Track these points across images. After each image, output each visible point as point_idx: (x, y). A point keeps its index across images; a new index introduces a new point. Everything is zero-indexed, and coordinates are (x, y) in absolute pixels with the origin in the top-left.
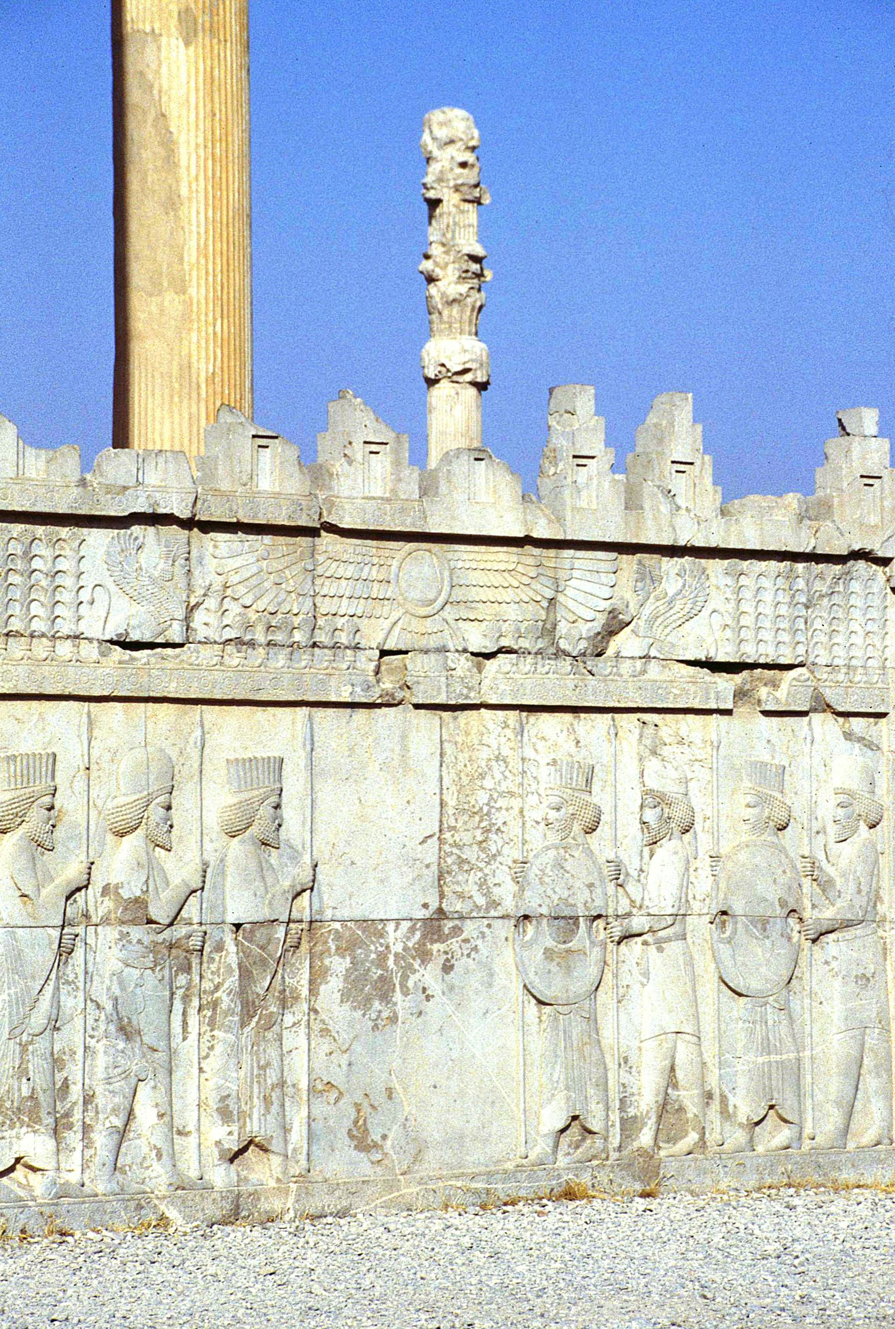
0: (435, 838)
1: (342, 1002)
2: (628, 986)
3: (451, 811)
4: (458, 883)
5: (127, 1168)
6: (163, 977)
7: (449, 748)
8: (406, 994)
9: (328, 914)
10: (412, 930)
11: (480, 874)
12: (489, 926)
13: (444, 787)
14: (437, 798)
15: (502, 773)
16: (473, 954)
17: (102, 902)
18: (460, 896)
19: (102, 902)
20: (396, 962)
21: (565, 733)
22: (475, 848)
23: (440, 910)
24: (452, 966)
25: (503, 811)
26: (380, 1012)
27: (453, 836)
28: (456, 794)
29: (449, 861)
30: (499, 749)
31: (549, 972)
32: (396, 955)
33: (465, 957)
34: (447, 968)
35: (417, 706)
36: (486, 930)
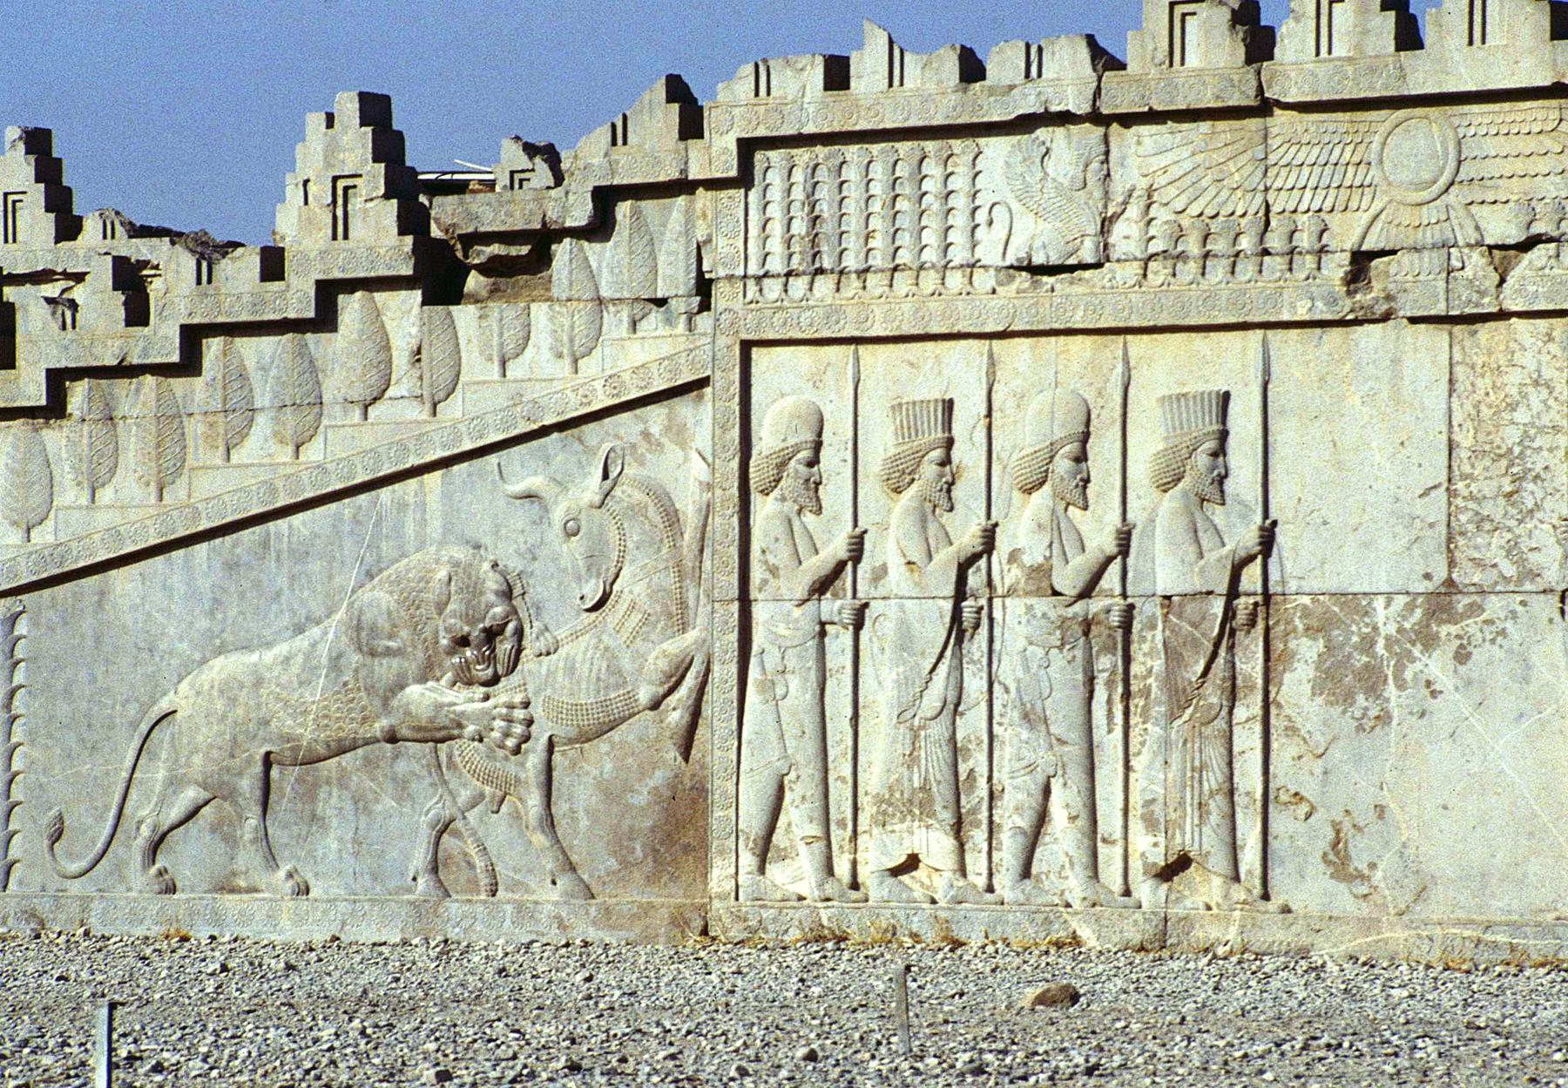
0: (1443, 489)
1: (1314, 694)
3: (1464, 454)
5: (1044, 877)
6: (1074, 657)
8: (1401, 685)
9: (1293, 586)
10: (1410, 607)
13: (1455, 423)
14: (1444, 438)
17: (1009, 570)
19: (1009, 570)
20: (1388, 647)
23: (1450, 582)
26: (1366, 709)
27: (1468, 486)
28: (1472, 432)
29: (1463, 518)
32: (1388, 638)
34: (1462, 656)
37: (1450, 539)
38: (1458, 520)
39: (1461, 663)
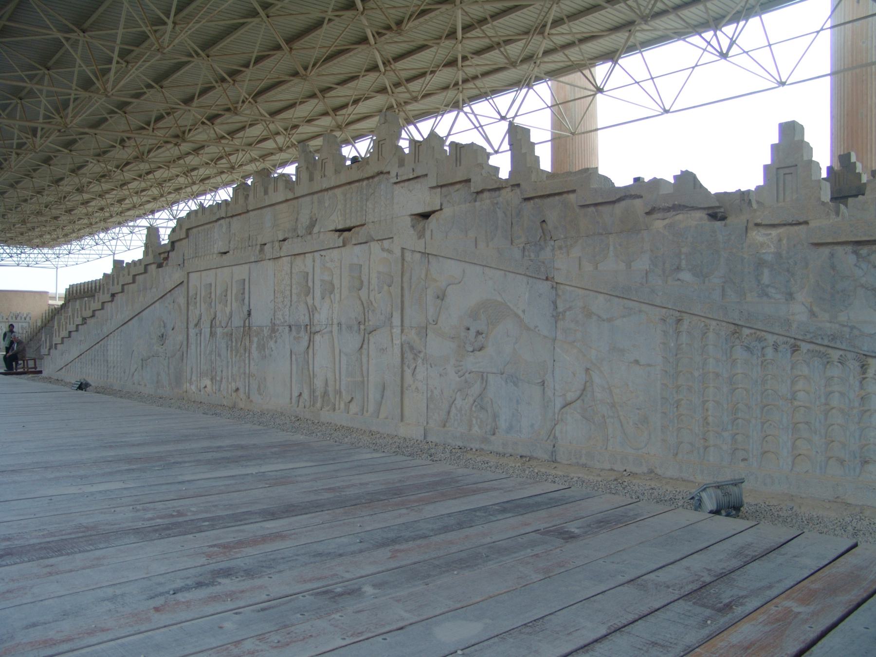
8: (268, 349)
10: (269, 329)
34: (276, 342)
35: (269, 259)
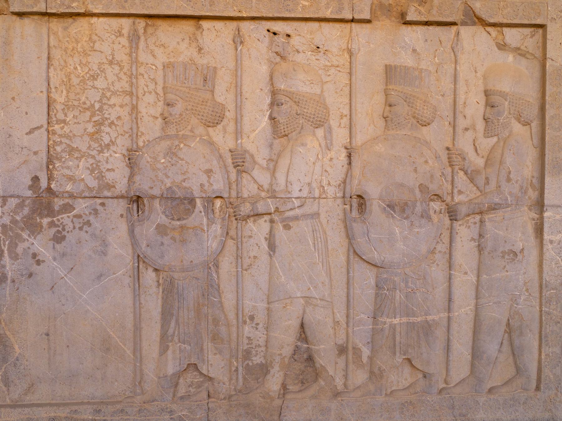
0: (43, 130)
2: (255, 257)
3: (59, 107)
4: (68, 168)
7: (57, 54)
11: (91, 161)
12: (103, 204)
13: (52, 86)
14: (44, 96)
15: (117, 75)
16: (86, 228)
18: (70, 179)
21: (187, 41)
22: (87, 138)
23: (49, 189)
24: (64, 238)
25: (117, 108)
27: (62, 128)
29: (59, 149)
30: (113, 55)
31: (162, 244)
33: (77, 230)
34: (59, 238)
36: (99, 208)
37: (50, 161)
38: (55, 150)
39: (58, 243)
